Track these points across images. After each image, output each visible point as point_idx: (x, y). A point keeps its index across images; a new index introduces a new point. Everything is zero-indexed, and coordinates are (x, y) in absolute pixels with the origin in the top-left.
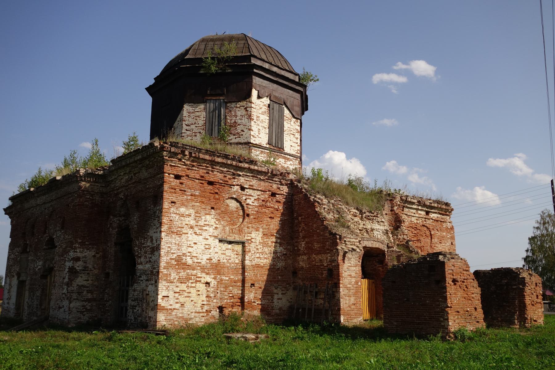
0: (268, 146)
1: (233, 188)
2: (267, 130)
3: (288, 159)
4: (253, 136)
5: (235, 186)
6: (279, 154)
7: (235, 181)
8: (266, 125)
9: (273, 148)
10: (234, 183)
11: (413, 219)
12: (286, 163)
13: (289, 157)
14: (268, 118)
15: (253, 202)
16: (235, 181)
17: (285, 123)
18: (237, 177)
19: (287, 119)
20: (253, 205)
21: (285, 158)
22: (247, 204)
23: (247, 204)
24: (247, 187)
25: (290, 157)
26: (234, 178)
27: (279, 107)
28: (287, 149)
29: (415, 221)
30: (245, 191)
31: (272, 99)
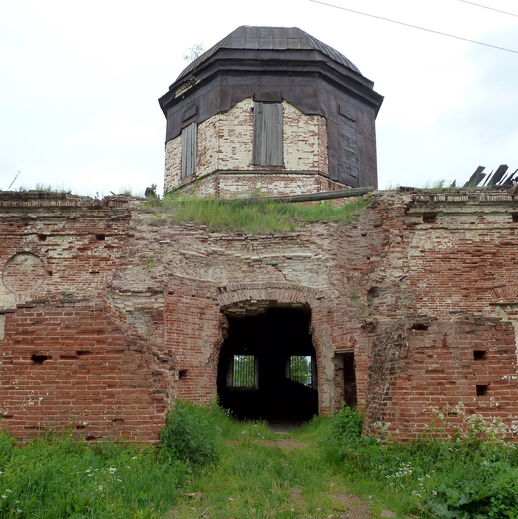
0: (251, 168)
1: (25, 239)
2: (251, 146)
3: (292, 180)
4: (222, 159)
5: (30, 236)
6: (274, 175)
7: (27, 229)
8: (248, 138)
9: (261, 169)
10: (26, 231)
11: (468, 235)
12: (288, 186)
13: (294, 176)
14: (251, 128)
15: (59, 254)
16: (27, 229)
17: (286, 128)
18: (31, 223)
19: (290, 120)
20: (61, 258)
21: (283, 179)
22: (51, 258)
23: (48, 258)
24: (49, 233)
25: (298, 176)
26: (26, 225)
27: (260, 105)
28: (291, 164)
29: (477, 239)
30: (46, 240)
31: (258, 98)
